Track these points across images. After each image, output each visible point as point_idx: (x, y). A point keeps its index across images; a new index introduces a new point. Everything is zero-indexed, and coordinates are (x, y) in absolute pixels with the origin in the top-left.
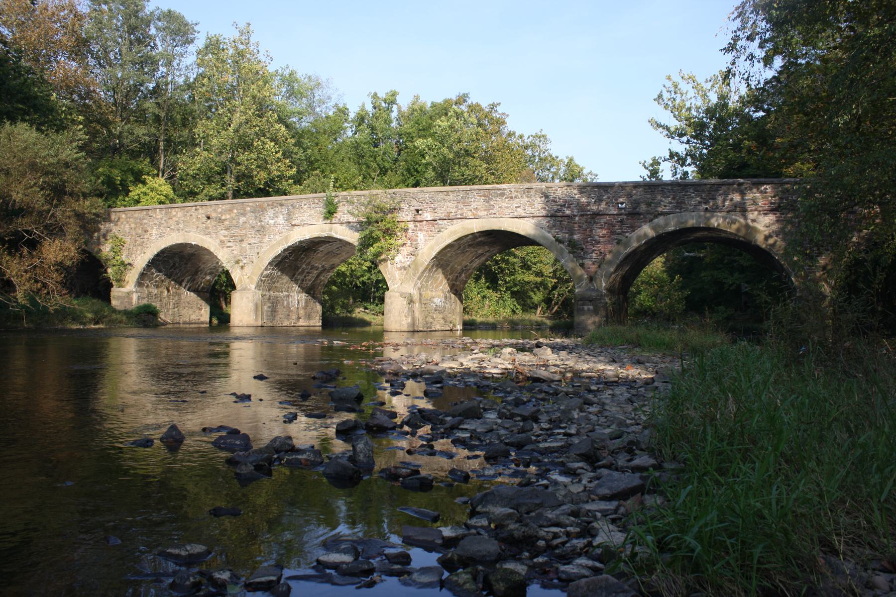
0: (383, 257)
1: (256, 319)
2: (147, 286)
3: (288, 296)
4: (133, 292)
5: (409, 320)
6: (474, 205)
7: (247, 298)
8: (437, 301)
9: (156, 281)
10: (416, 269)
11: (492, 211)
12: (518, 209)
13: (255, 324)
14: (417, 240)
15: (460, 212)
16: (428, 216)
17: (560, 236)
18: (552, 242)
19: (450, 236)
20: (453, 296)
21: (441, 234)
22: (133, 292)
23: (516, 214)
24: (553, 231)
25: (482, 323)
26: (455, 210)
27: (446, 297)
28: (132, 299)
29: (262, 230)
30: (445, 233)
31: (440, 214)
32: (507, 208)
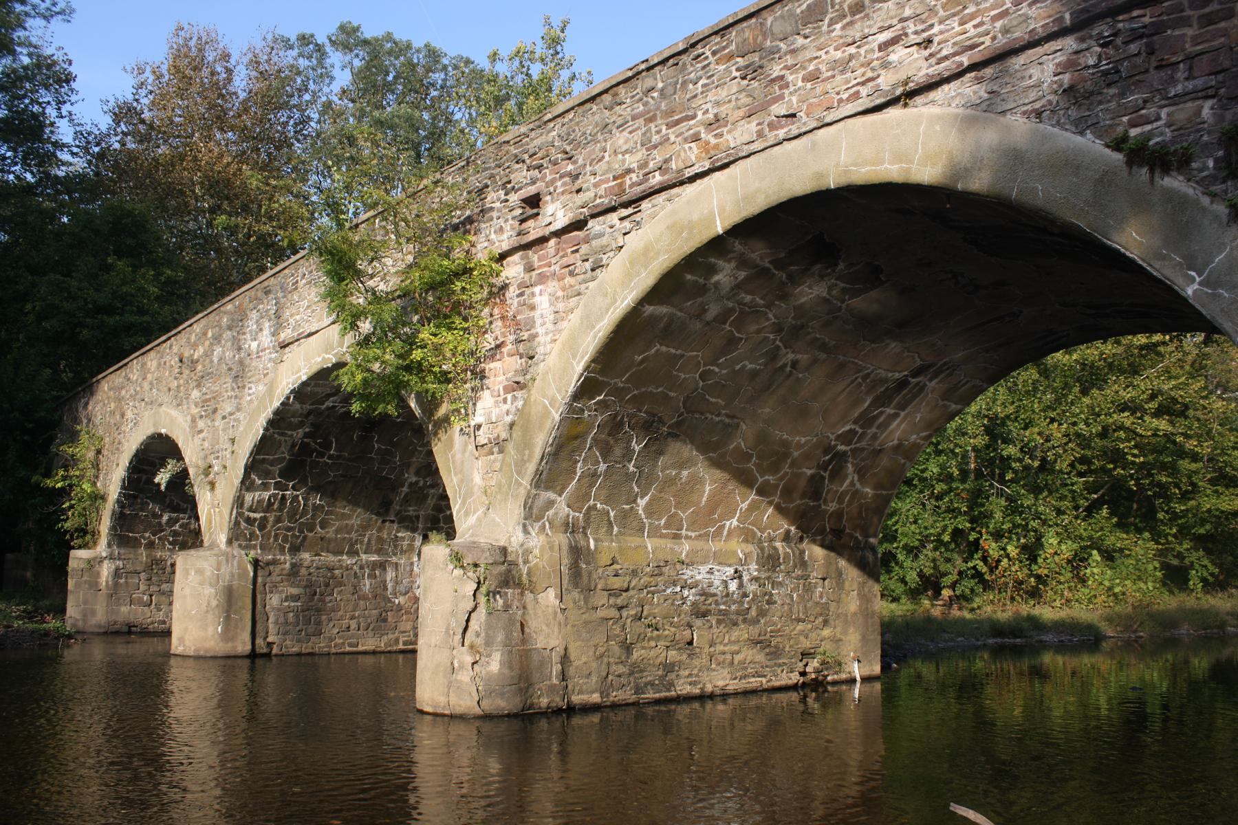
0: (443, 410)
1: (227, 635)
2: (151, 545)
3: (382, 566)
4: (101, 560)
5: (494, 664)
6: (706, 109)
7: (200, 572)
8: (714, 576)
9: (175, 534)
10: (526, 444)
11: (779, 109)
12: (898, 54)
13: (221, 648)
14: (531, 323)
15: (658, 157)
16: (556, 213)
17: (1159, 127)
18: (1105, 180)
19: (629, 275)
20: (816, 553)
21: (601, 275)
22: (101, 560)
23: (886, 81)
24: (1102, 113)
25: (1059, 627)
26: (641, 154)
27: (770, 561)
28: (98, 575)
29: (240, 374)
30: (616, 265)
31: (596, 190)
32: (843, 66)
